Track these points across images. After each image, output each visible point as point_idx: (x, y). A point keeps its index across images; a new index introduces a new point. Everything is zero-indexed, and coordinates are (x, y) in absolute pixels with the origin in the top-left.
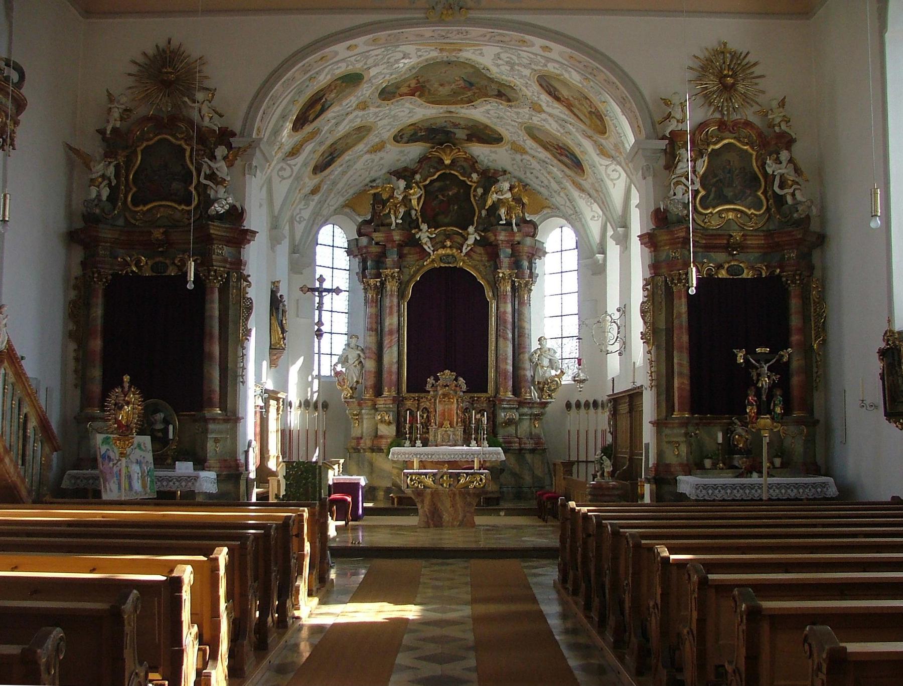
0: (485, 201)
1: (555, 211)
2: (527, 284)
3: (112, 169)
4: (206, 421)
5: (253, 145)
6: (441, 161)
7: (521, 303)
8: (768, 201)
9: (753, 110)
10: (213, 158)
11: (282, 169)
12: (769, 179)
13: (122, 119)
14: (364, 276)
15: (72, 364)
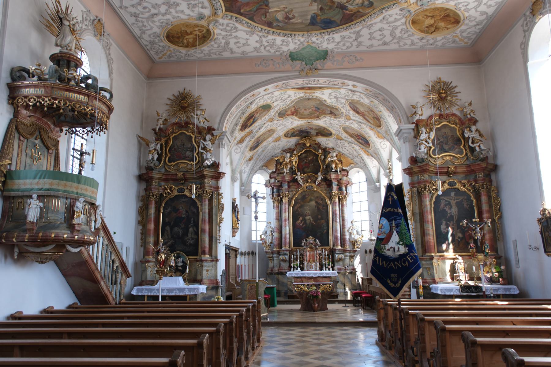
0: (325, 162)
1: (356, 165)
2: (345, 197)
3: (158, 147)
4: (202, 261)
5: (223, 134)
6: (305, 145)
7: (343, 206)
8: (466, 150)
10: (205, 140)
11: (236, 149)
12: (467, 140)
13: (163, 124)
14: (273, 196)
15: (140, 236)
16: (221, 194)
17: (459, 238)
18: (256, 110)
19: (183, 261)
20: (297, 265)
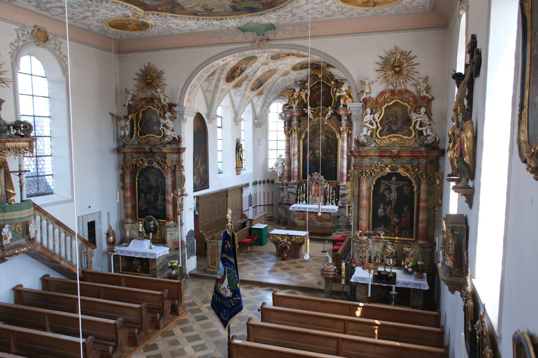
3: (128, 123)
6: (317, 76)
8: (415, 132)
9: (410, 83)
10: (165, 118)
11: (236, 92)
13: (132, 100)
16: (182, 167)
17: (395, 222)
18: (239, 63)
19: (154, 224)
20: (303, 198)
